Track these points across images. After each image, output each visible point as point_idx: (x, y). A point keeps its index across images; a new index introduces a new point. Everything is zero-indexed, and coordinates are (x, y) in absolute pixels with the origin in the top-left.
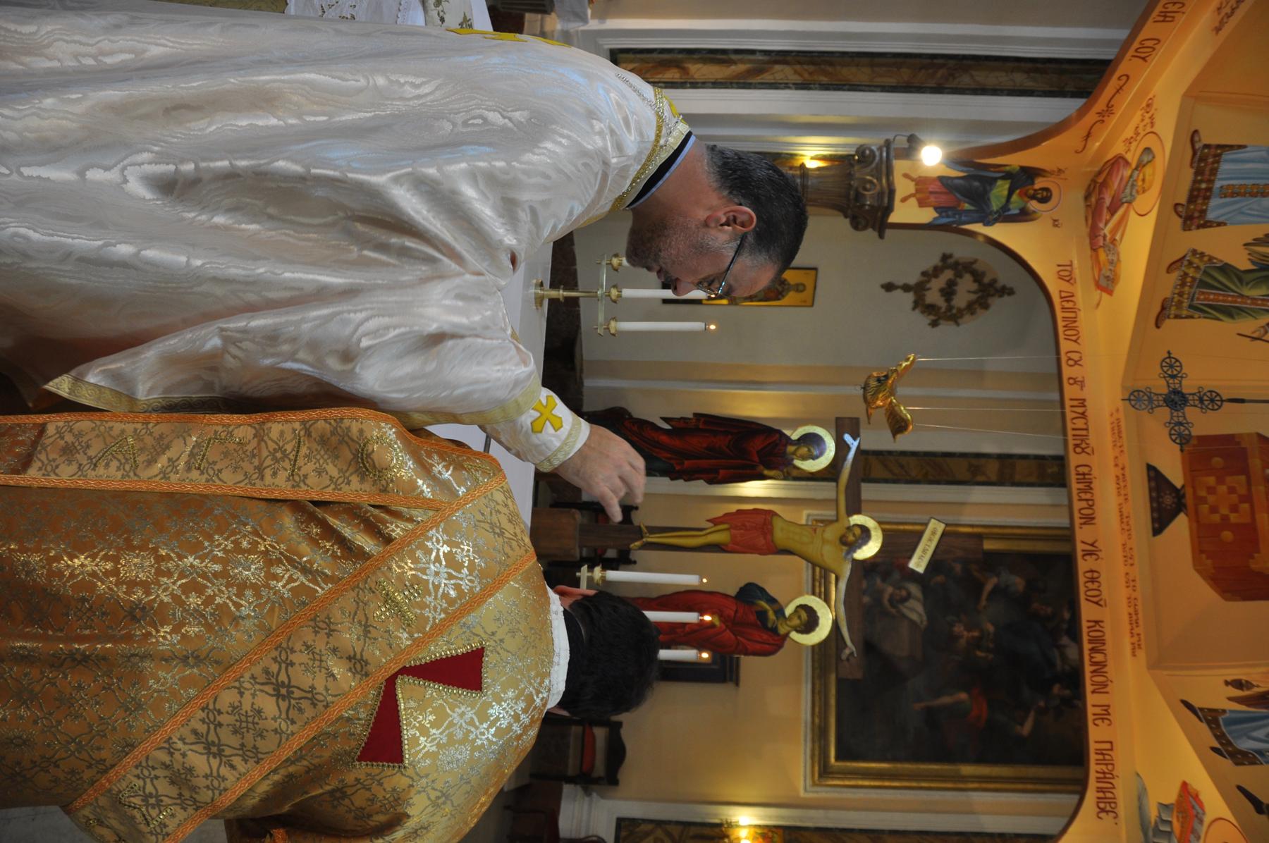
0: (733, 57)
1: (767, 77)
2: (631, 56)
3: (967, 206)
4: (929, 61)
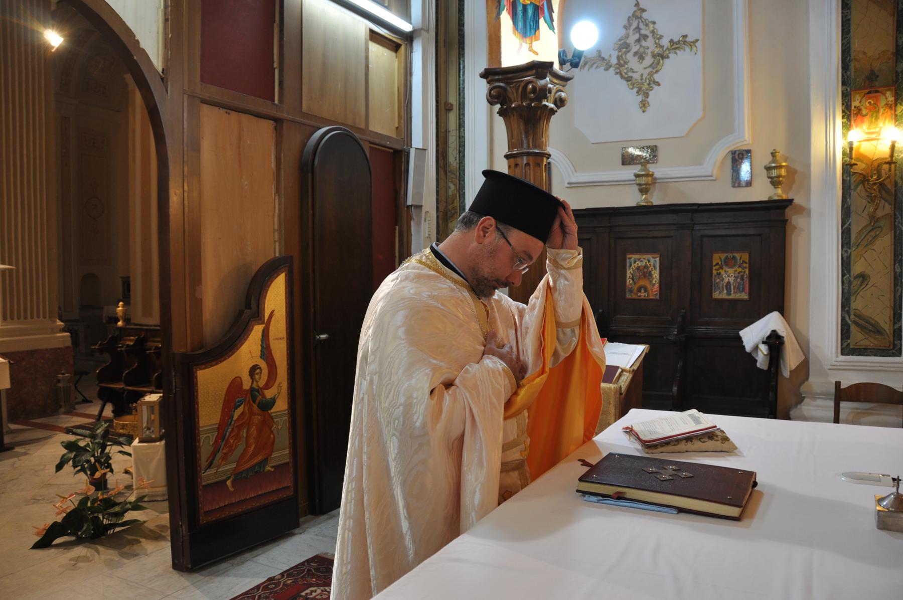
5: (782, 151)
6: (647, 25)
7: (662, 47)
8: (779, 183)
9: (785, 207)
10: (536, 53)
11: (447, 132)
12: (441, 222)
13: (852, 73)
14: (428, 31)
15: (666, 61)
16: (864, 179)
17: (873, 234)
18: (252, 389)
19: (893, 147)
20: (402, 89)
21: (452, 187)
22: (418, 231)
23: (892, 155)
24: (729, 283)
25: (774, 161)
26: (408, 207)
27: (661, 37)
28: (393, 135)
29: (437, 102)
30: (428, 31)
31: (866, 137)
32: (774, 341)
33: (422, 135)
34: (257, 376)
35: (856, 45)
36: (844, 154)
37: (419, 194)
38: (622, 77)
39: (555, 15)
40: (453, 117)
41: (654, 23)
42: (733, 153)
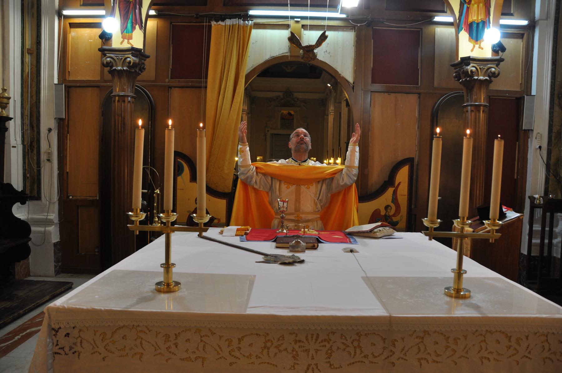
12: (553, 138)
18: (385, 215)
26: (525, 130)
34: (389, 210)
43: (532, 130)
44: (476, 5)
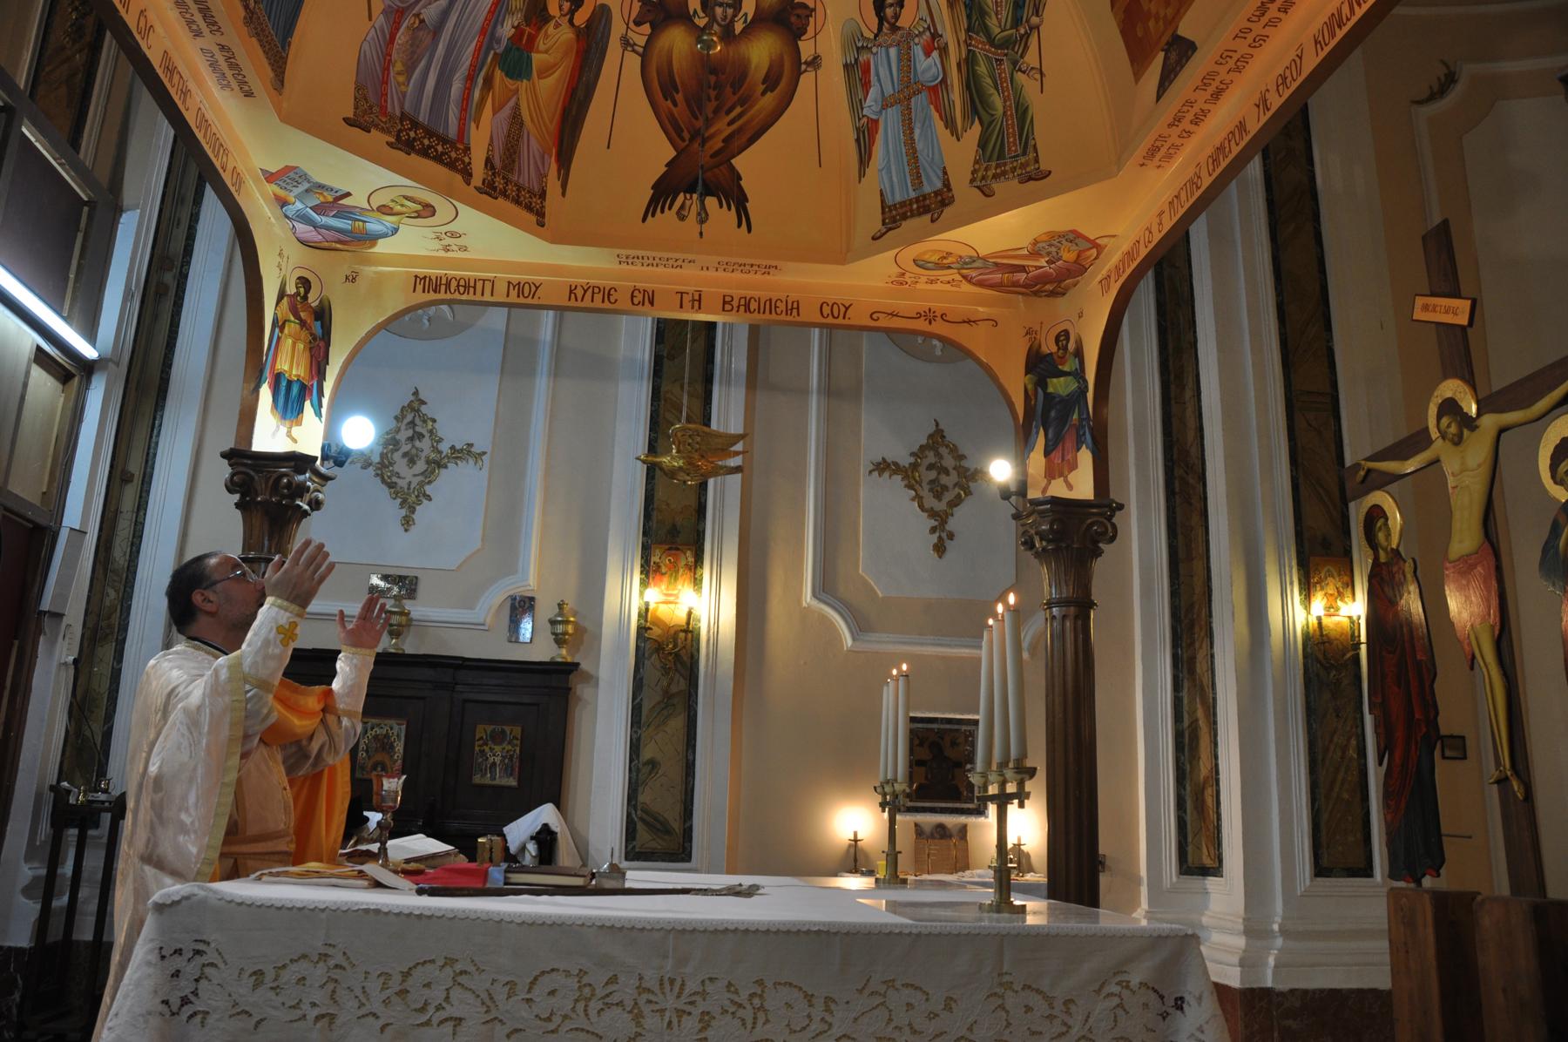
0: (1186, 723)
1: (1206, 681)
2: (1190, 849)
3: (1075, 416)
4: (1178, 500)
5: (571, 604)
6: (425, 422)
7: (440, 452)
8: (565, 642)
9: (570, 672)
10: (295, 441)
11: (117, 512)
13: (654, 524)
14: (118, 365)
15: (443, 471)
16: (659, 647)
17: (665, 712)
19: (690, 614)
20: (64, 438)
21: (112, 594)
22: (50, 653)
23: (688, 623)
24: (494, 764)
25: (560, 614)
27: (441, 440)
28: (36, 501)
29: (112, 466)
30: (118, 365)
31: (662, 598)
32: (545, 838)
33: (80, 507)
35: (660, 494)
36: (640, 615)
37: (62, 596)
38: (383, 481)
39: (325, 401)
40: (130, 495)
41: (434, 421)
42: (513, 598)
43: (59, 616)
44: (290, 341)
